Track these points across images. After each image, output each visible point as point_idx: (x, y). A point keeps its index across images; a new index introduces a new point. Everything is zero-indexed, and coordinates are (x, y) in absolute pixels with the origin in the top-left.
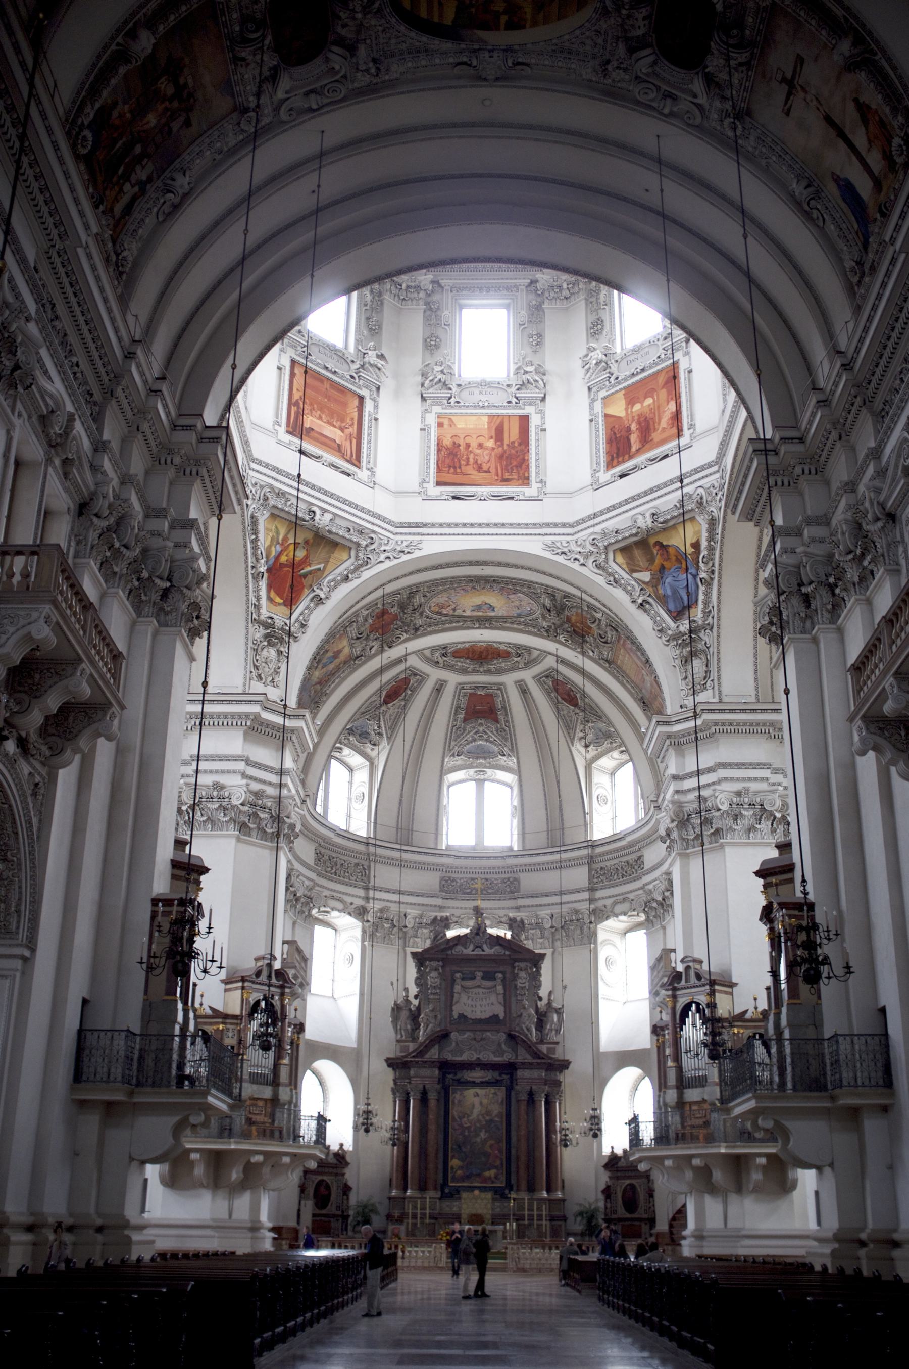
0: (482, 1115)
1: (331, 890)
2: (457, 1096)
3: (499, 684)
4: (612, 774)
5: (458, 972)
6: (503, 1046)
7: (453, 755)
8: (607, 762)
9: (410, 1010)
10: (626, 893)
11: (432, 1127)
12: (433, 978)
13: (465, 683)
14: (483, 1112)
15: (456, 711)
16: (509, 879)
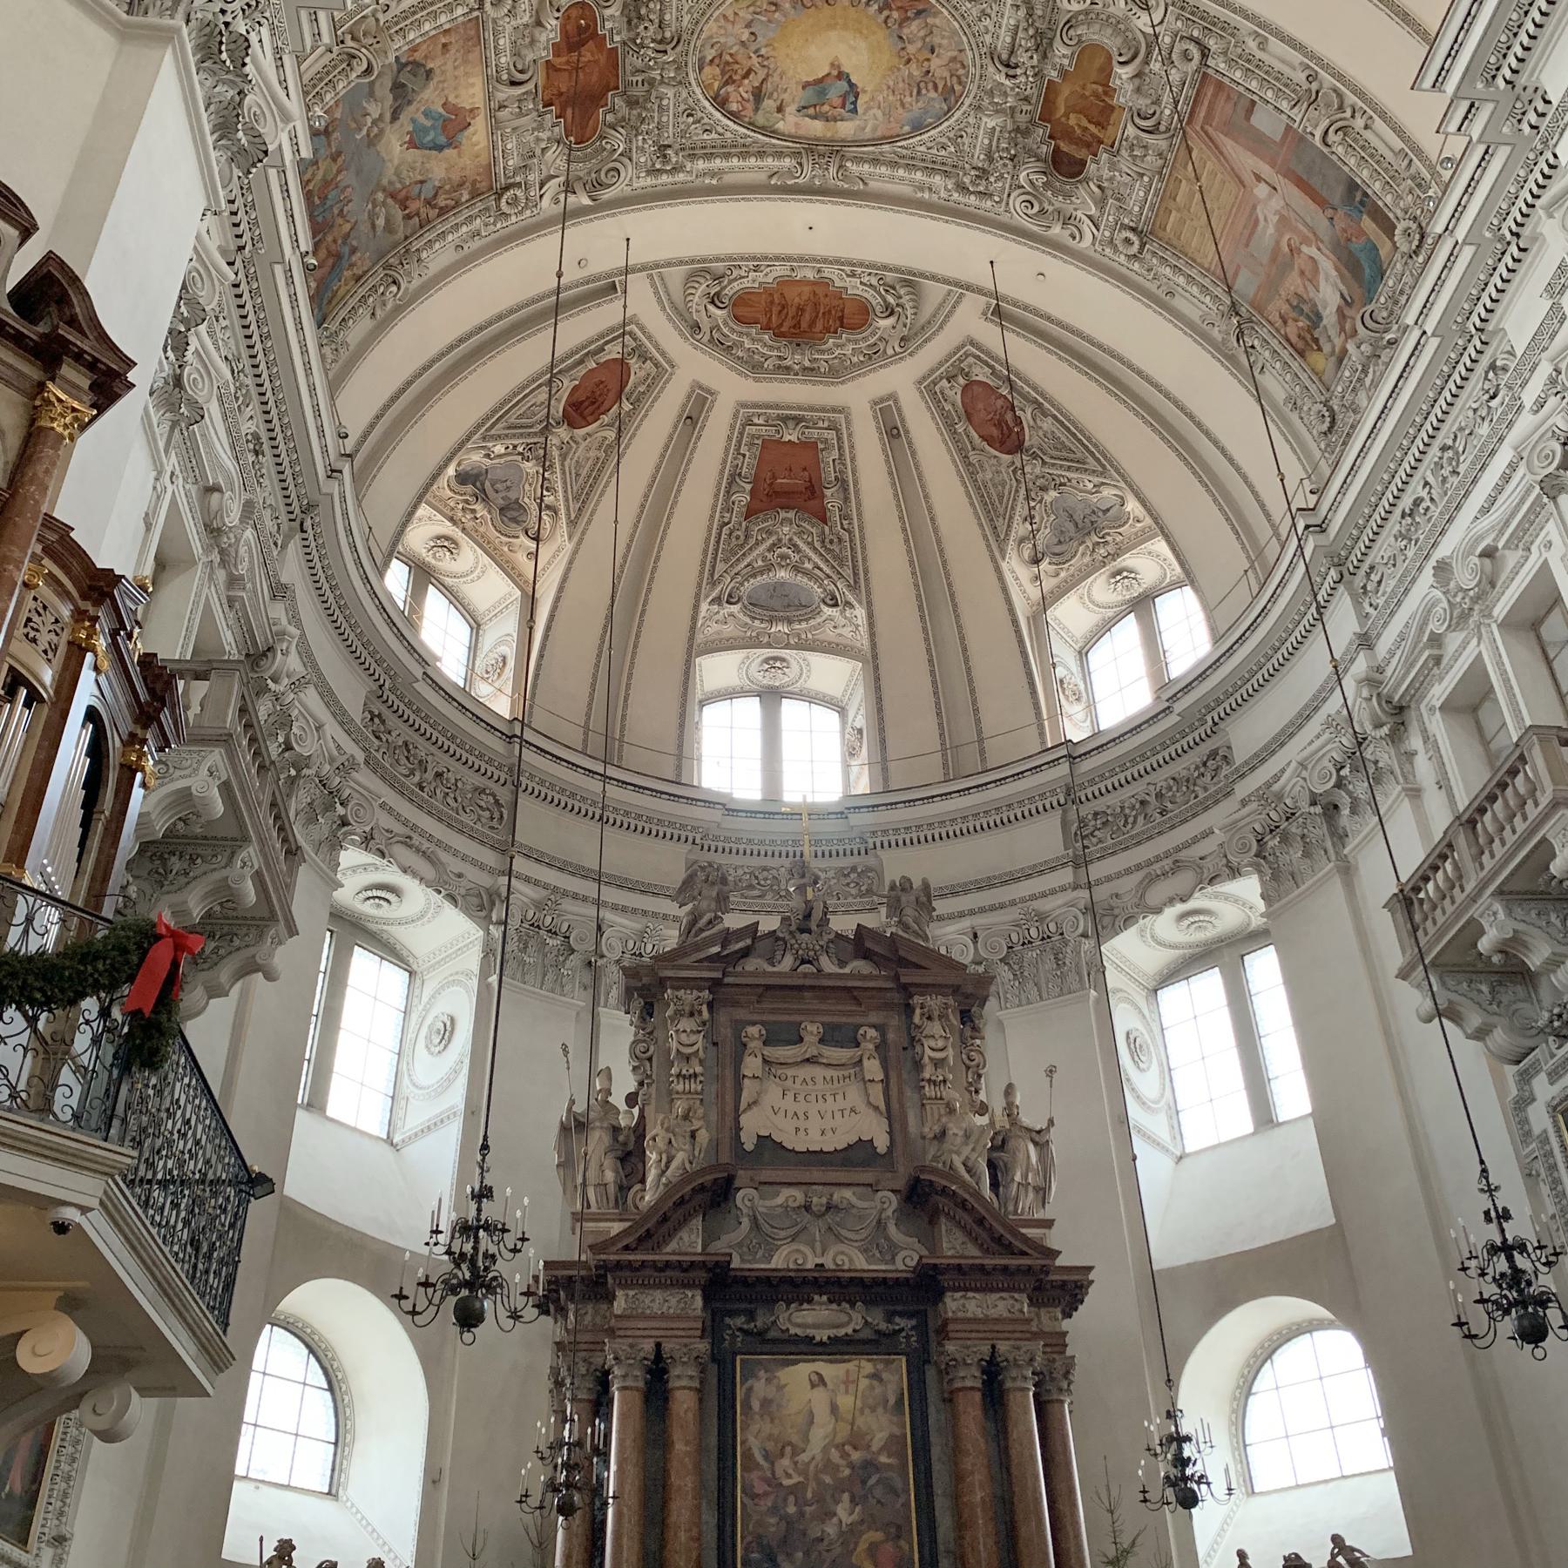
0: (840, 1447)
1: (405, 823)
2: (760, 1387)
3: (834, 410)
4: (1083, 654)
5: (754, 1024)
6: (892, 1229)
7: (717, 600)
8: (1071, 615)
9: (616, 1130)
10: (1178, 849)
11: (683, 1481)
12: (683, 1035)
13: (756, 406)
14: (844, 1431)
15: (730, 484)
16: (854, 869)
